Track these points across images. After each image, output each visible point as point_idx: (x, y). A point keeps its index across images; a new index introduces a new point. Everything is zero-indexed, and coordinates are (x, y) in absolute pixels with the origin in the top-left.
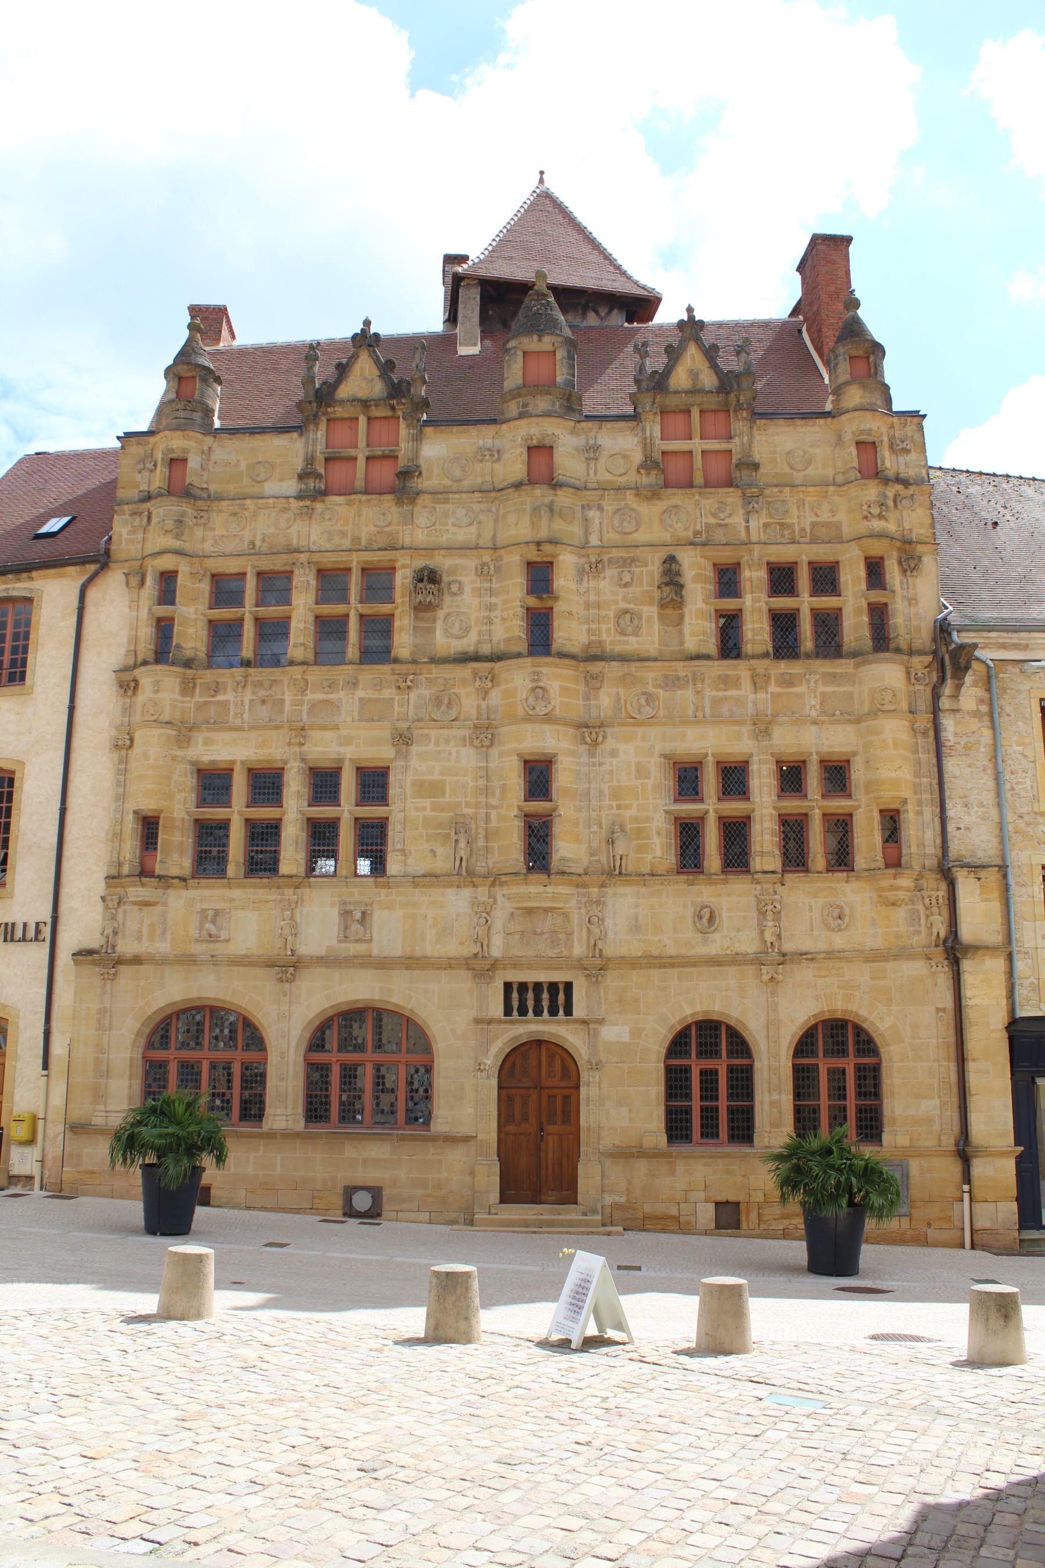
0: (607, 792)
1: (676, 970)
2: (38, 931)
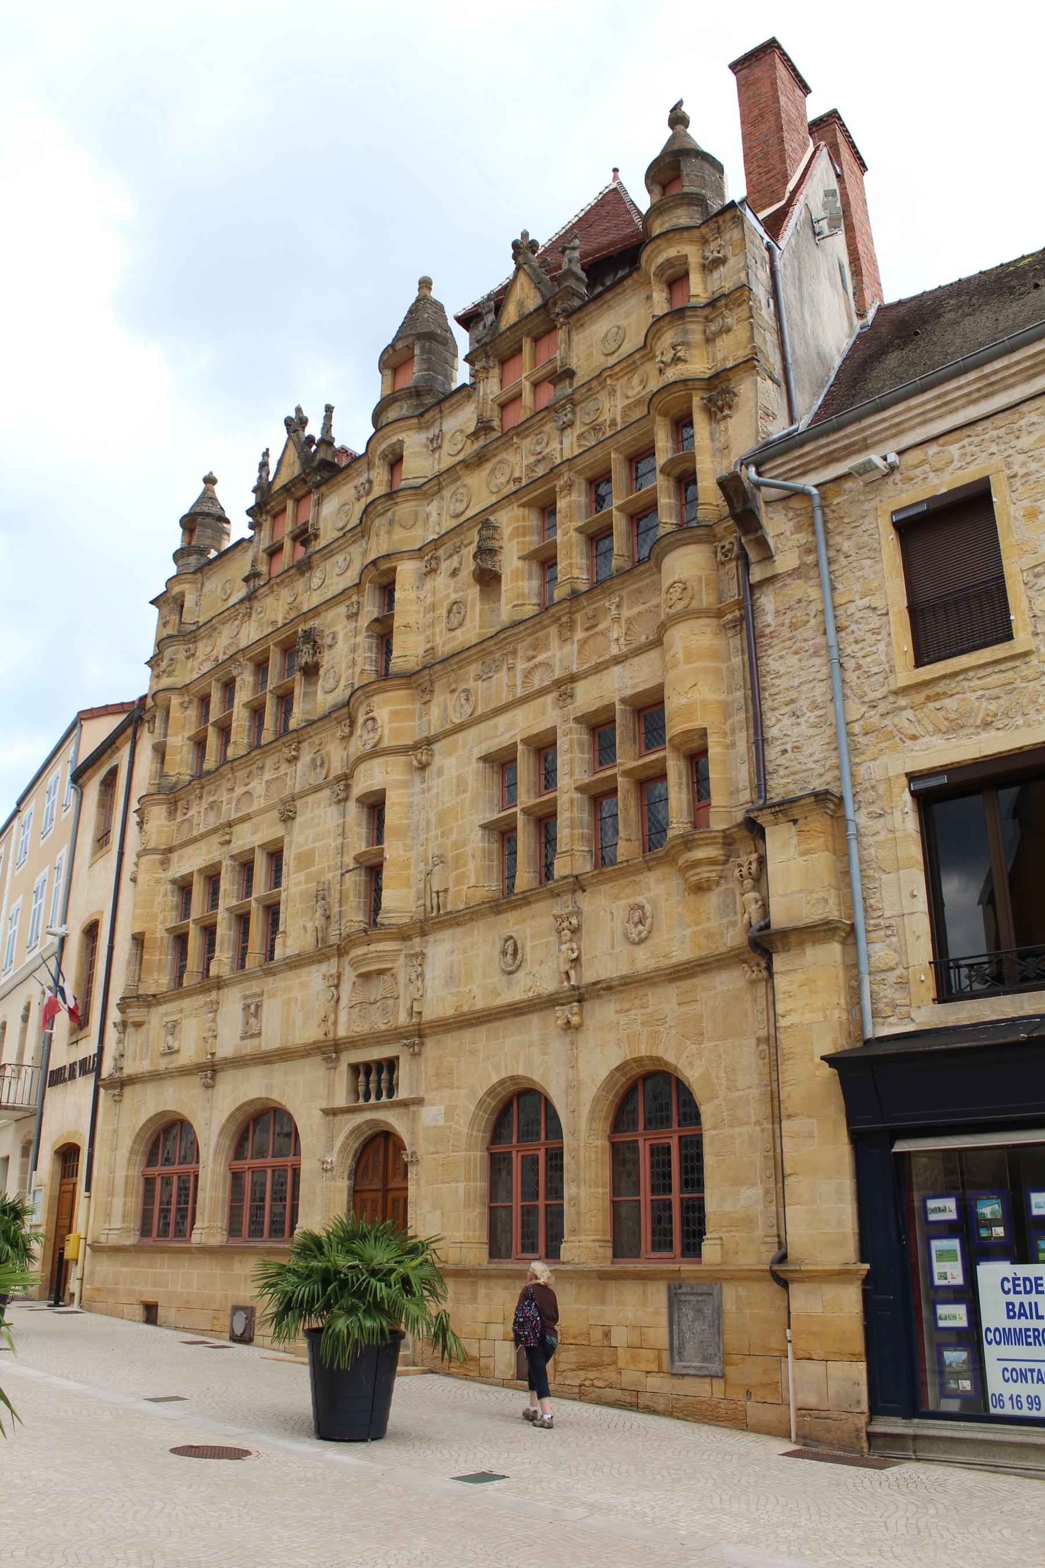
0: (433, 821)
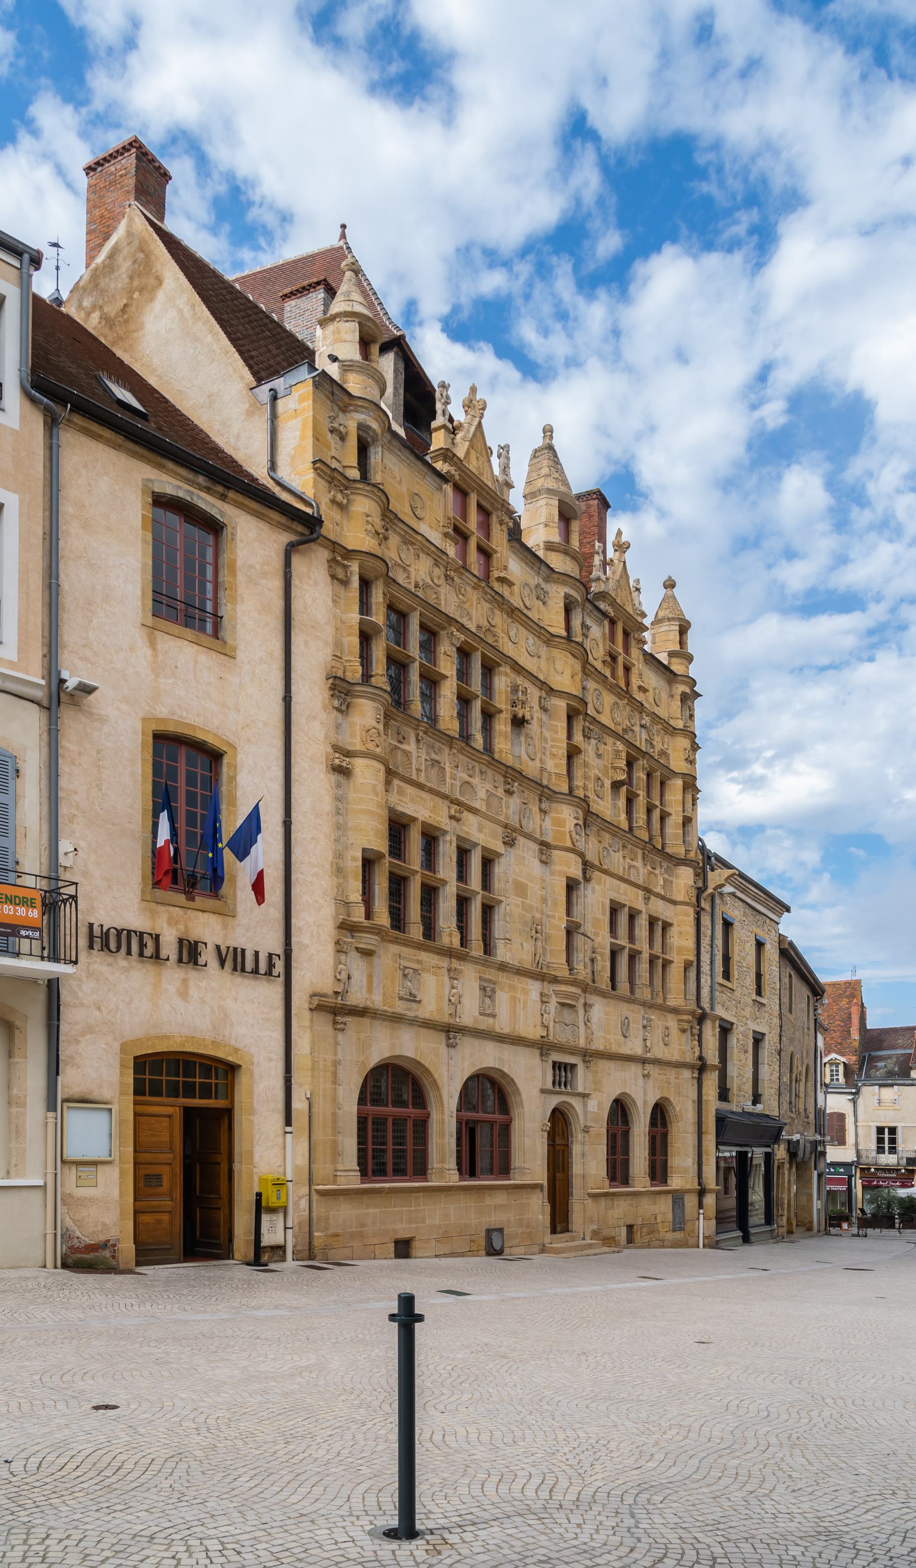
2: (271, 966)
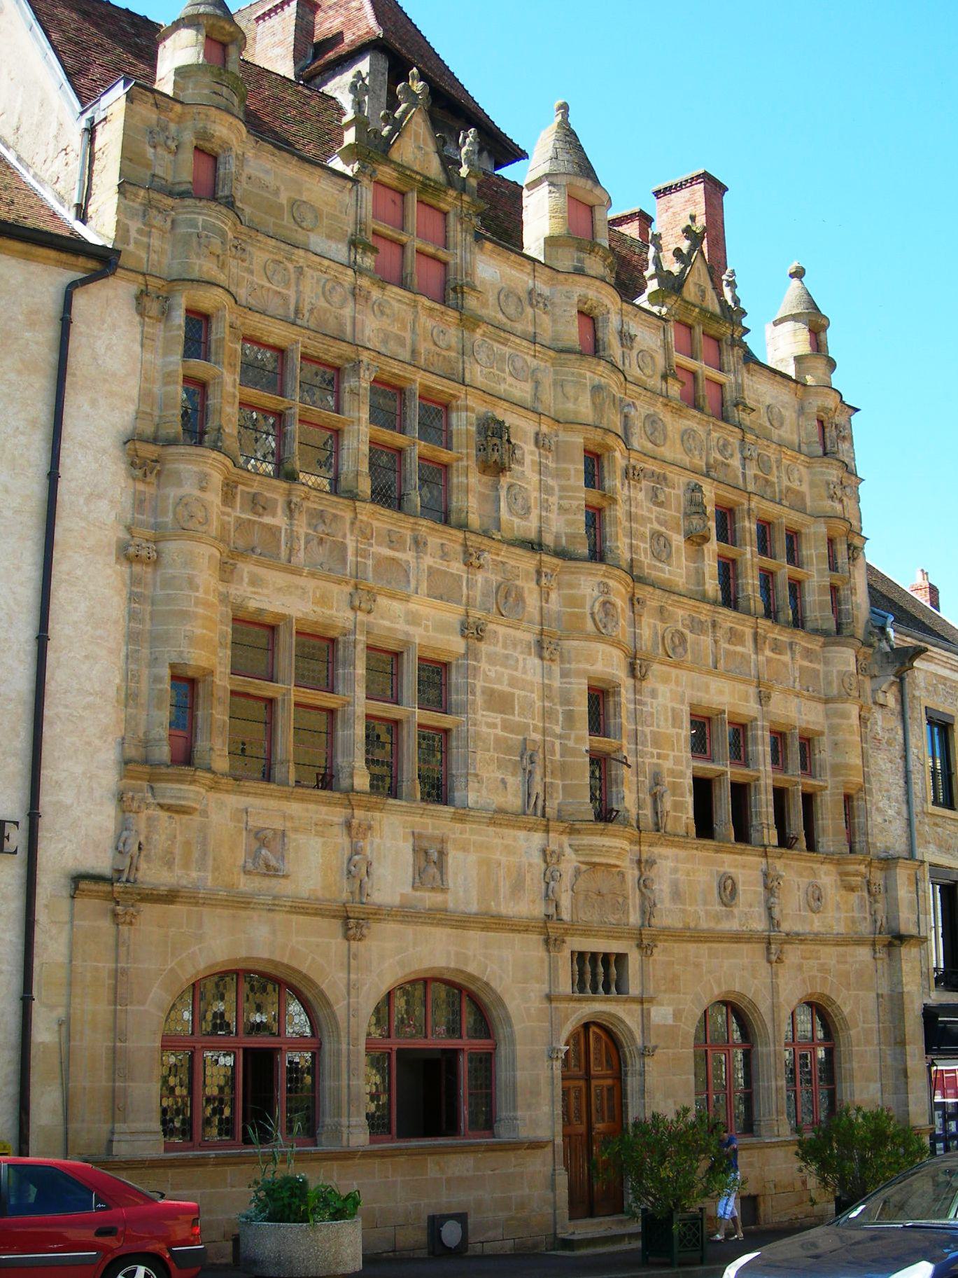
1: (706, 945)
